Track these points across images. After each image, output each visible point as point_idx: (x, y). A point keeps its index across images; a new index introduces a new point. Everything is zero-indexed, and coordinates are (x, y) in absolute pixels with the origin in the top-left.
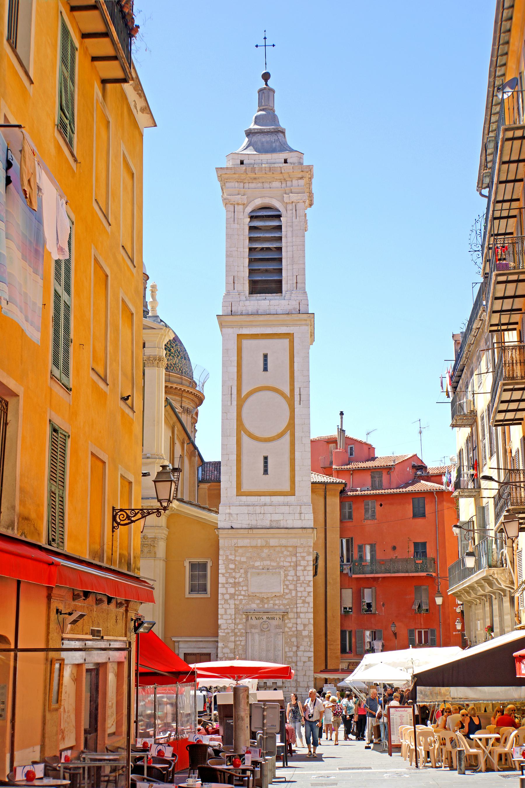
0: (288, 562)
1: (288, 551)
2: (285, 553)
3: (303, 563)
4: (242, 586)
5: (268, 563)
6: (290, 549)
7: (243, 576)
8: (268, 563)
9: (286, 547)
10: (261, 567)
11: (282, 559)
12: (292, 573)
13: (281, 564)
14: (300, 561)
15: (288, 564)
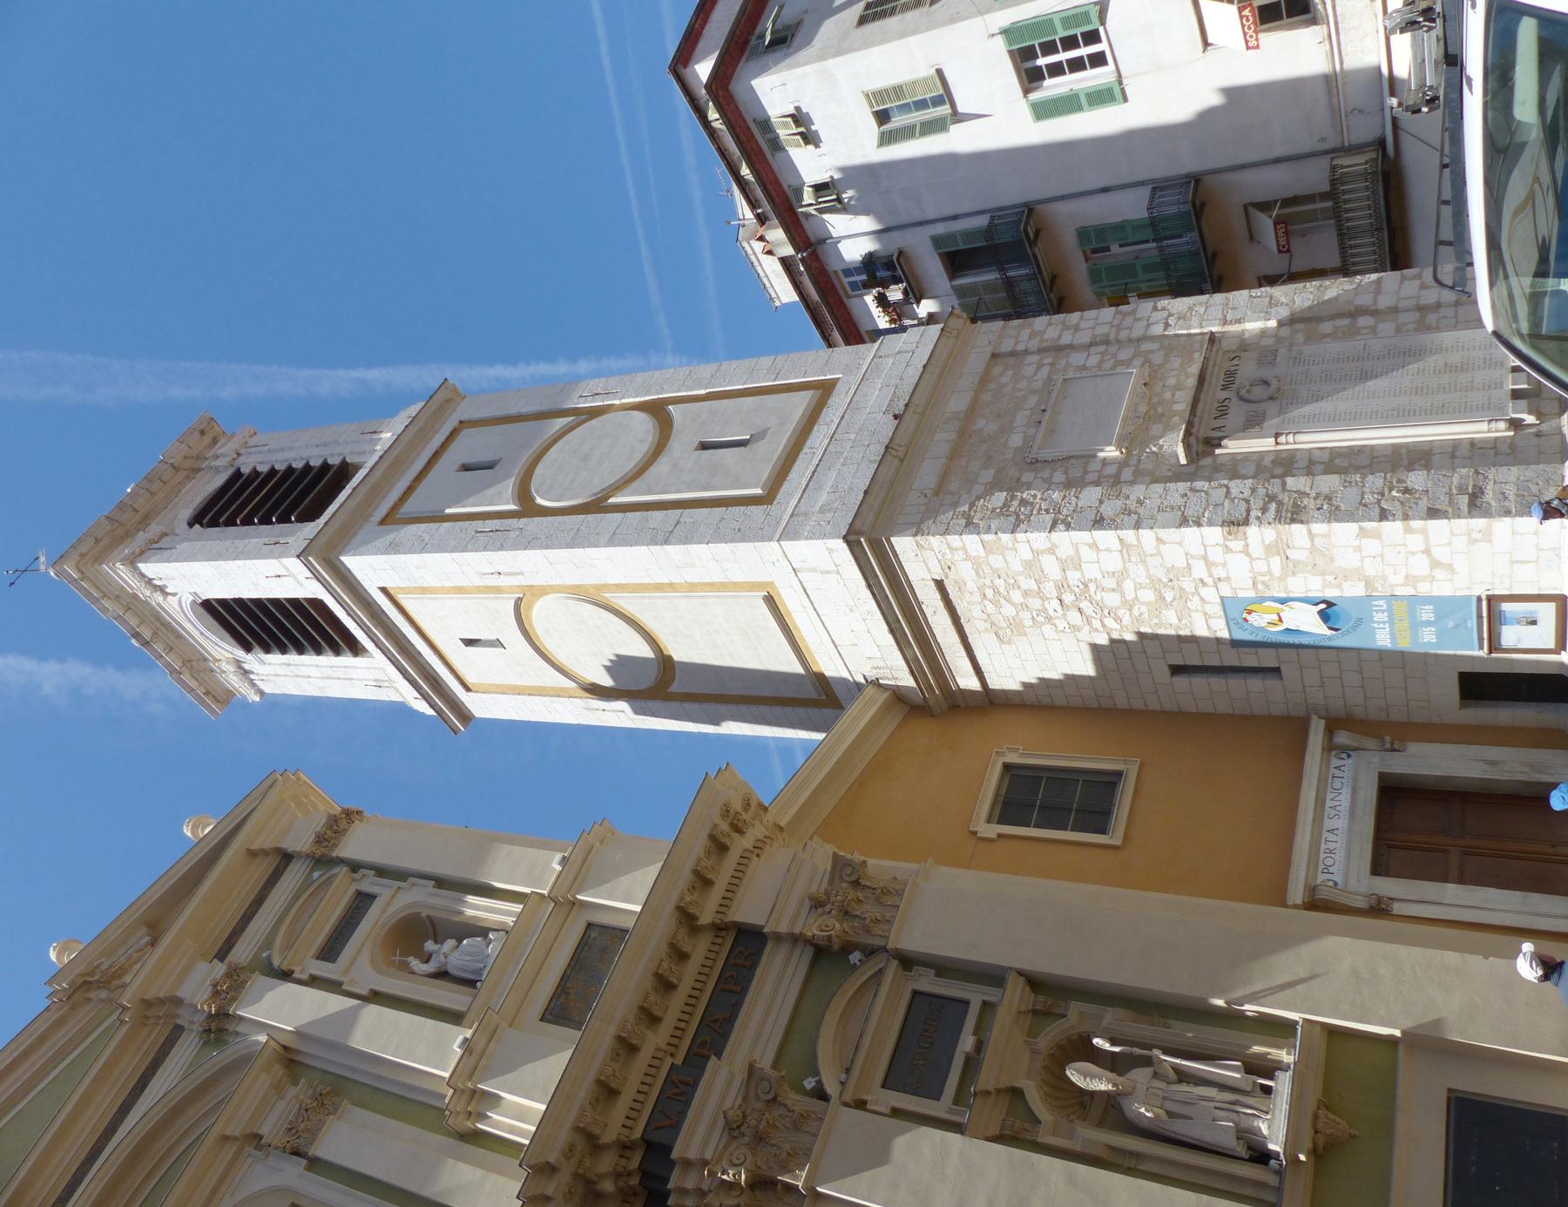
0: (1037, 370)
1: (1002, 374)
2: (1003, 380)
3: (1052, 333)
4: (1086, 472)
5: (1021, 418)
6: (997, 370)
7: (1046, 474)
8: (1021, 418)
9: (984, 380)
10: (1033, 431)
11: (1024, 384)
12: (1077, 358)
13: (1038, 384)
14: (1043, 341)
15: (1045, 371)
